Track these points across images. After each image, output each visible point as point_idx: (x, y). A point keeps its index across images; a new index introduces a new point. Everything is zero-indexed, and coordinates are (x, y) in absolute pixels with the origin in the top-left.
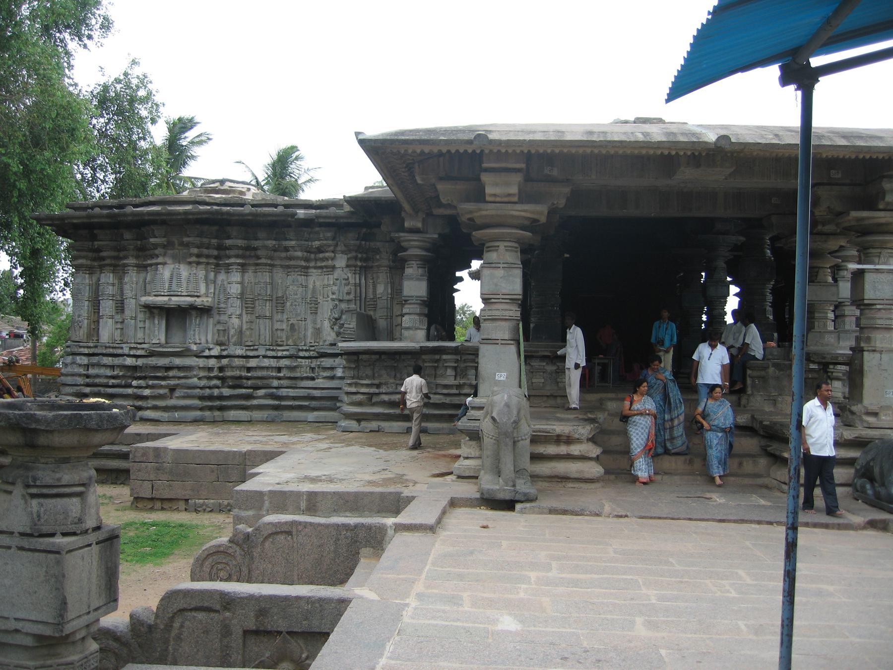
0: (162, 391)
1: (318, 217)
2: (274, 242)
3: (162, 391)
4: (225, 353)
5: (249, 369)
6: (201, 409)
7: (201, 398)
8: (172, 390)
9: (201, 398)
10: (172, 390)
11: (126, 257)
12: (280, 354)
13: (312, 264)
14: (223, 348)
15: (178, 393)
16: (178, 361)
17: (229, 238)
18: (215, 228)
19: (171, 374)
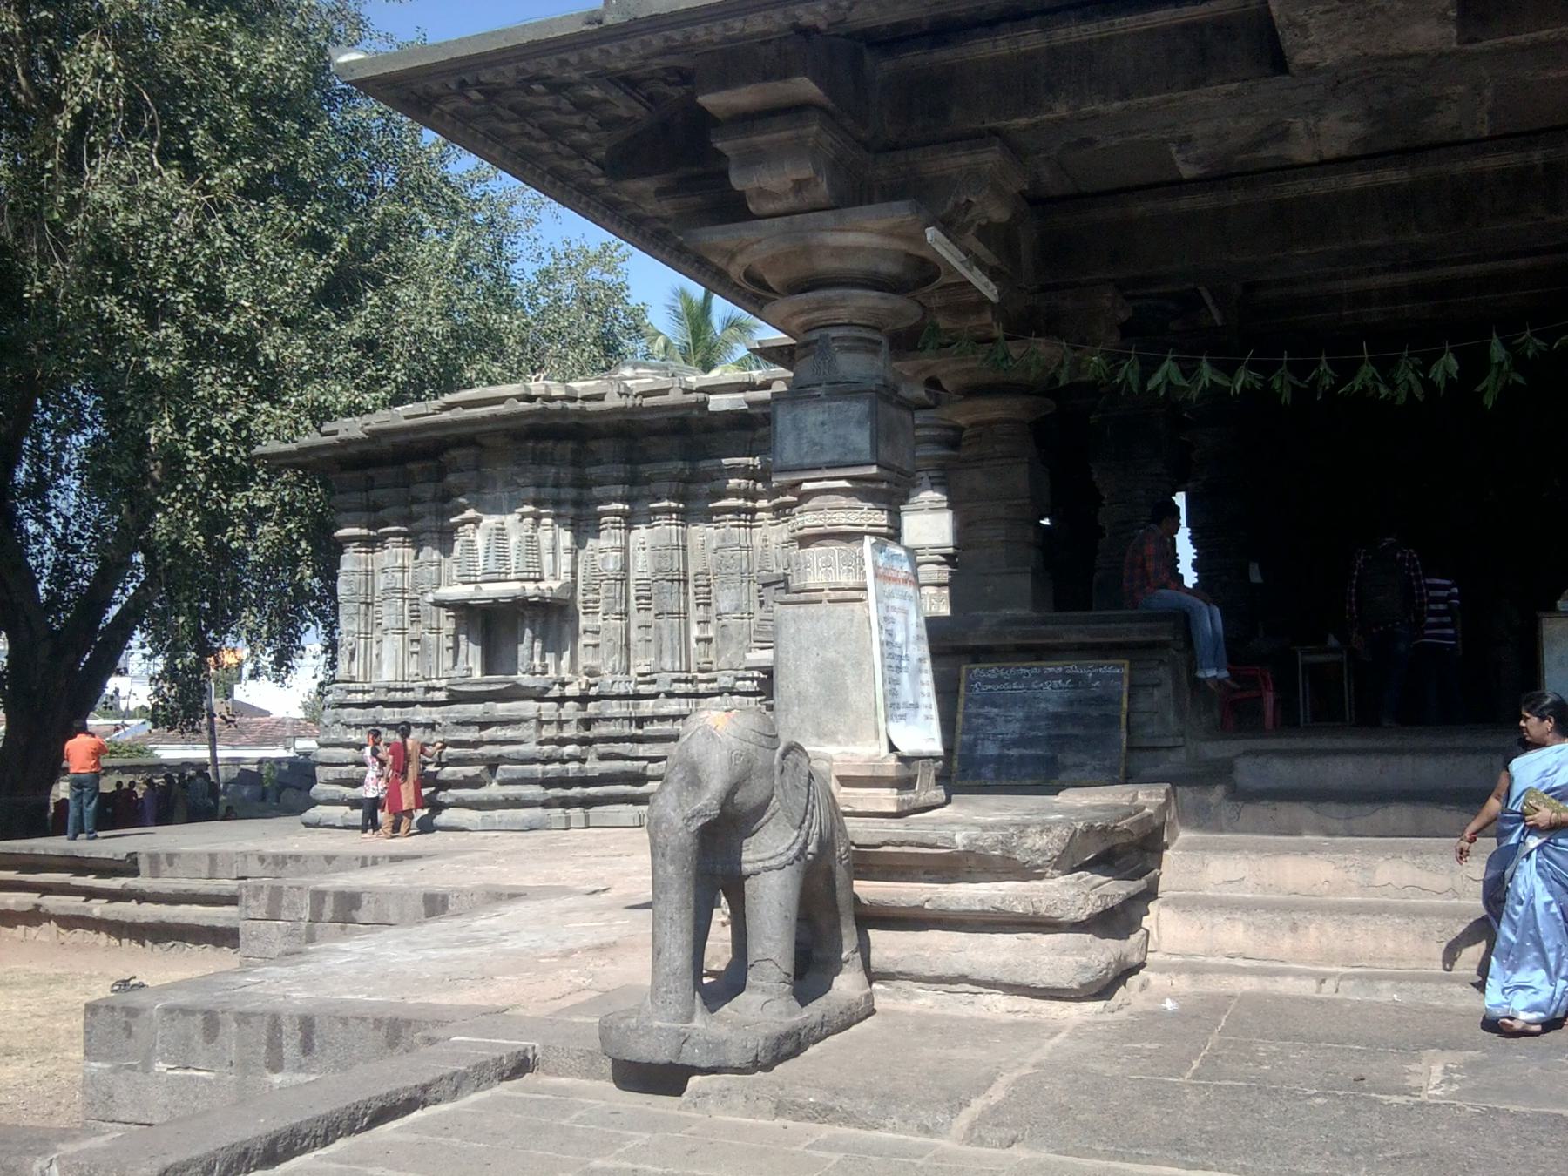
0: (471, 771)
1: (751, 404)
2: (680, 464)
3: (471, 771)
4: (593, 691)
5: (640, 721)
6: (546, 805)
7: (547, 783)
8: (492, 764)
9: (547, 783)
10: (492, 764)
11: (421, 517)
12: (702, 688)
13: (763, 503)
14: (591, 680)
15: (504, 770)
16: (501, 709)
17: (599, 462)
18: (570, 445)
19: (487, 734)
